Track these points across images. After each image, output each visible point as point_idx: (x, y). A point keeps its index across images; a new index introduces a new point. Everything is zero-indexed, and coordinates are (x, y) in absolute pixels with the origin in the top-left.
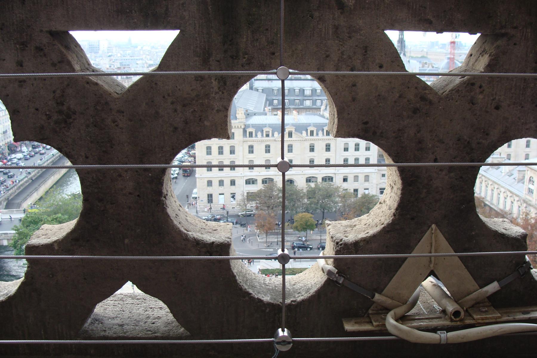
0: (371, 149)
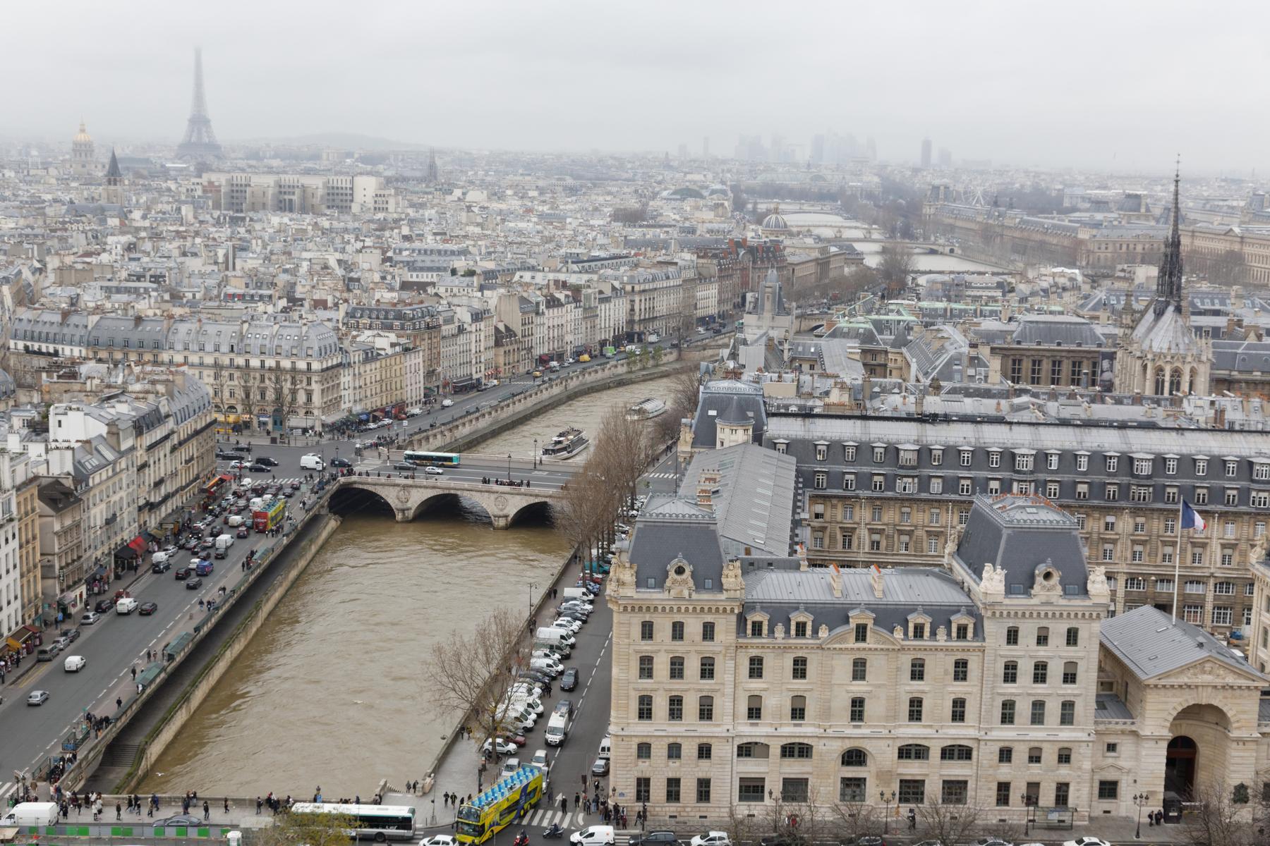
0: (1078, 678)
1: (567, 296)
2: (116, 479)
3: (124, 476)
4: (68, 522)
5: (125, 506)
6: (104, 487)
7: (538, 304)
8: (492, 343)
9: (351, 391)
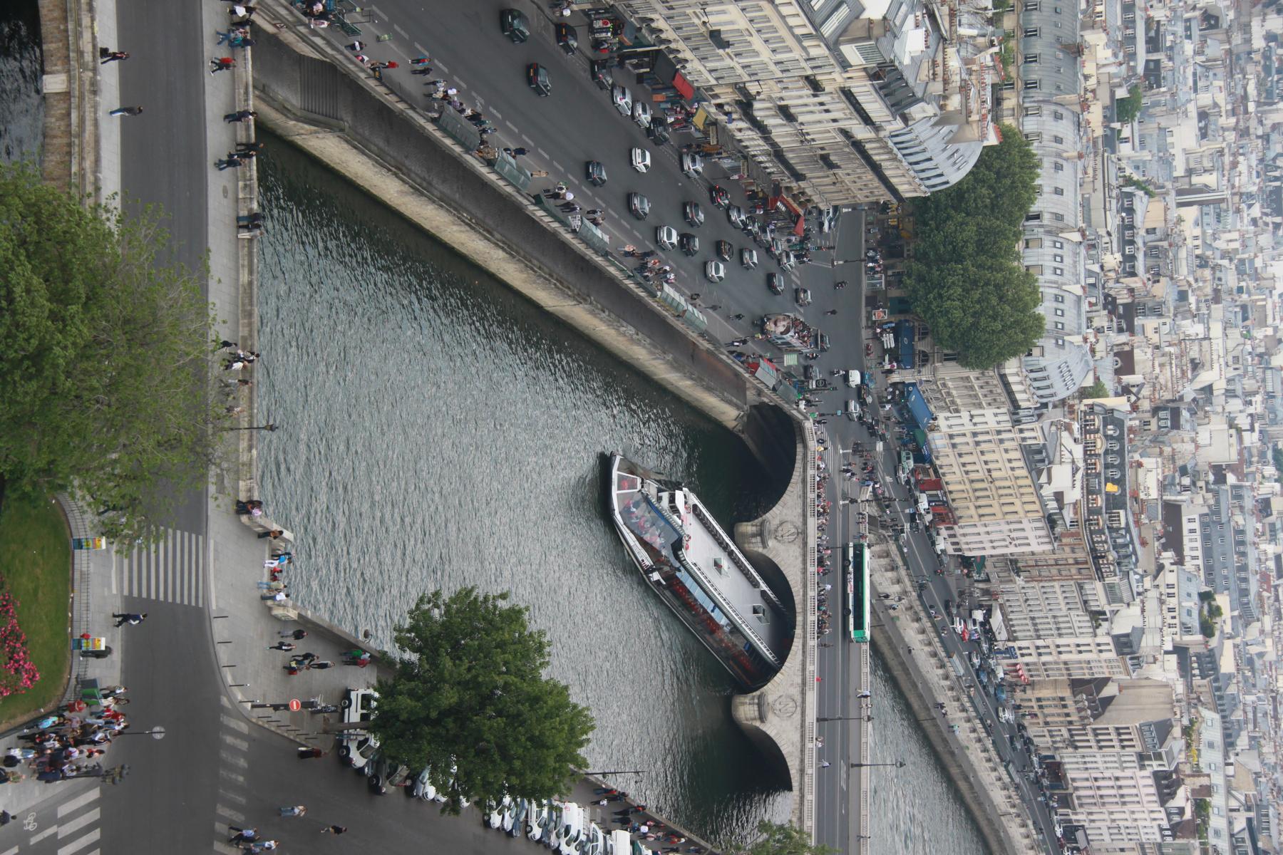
1: (1181, 811)
2: (791, 42)
3: (797, 54)
5: (745, 61)
6: (776, 21)
8: (1077, 675)
9: (969, 428)
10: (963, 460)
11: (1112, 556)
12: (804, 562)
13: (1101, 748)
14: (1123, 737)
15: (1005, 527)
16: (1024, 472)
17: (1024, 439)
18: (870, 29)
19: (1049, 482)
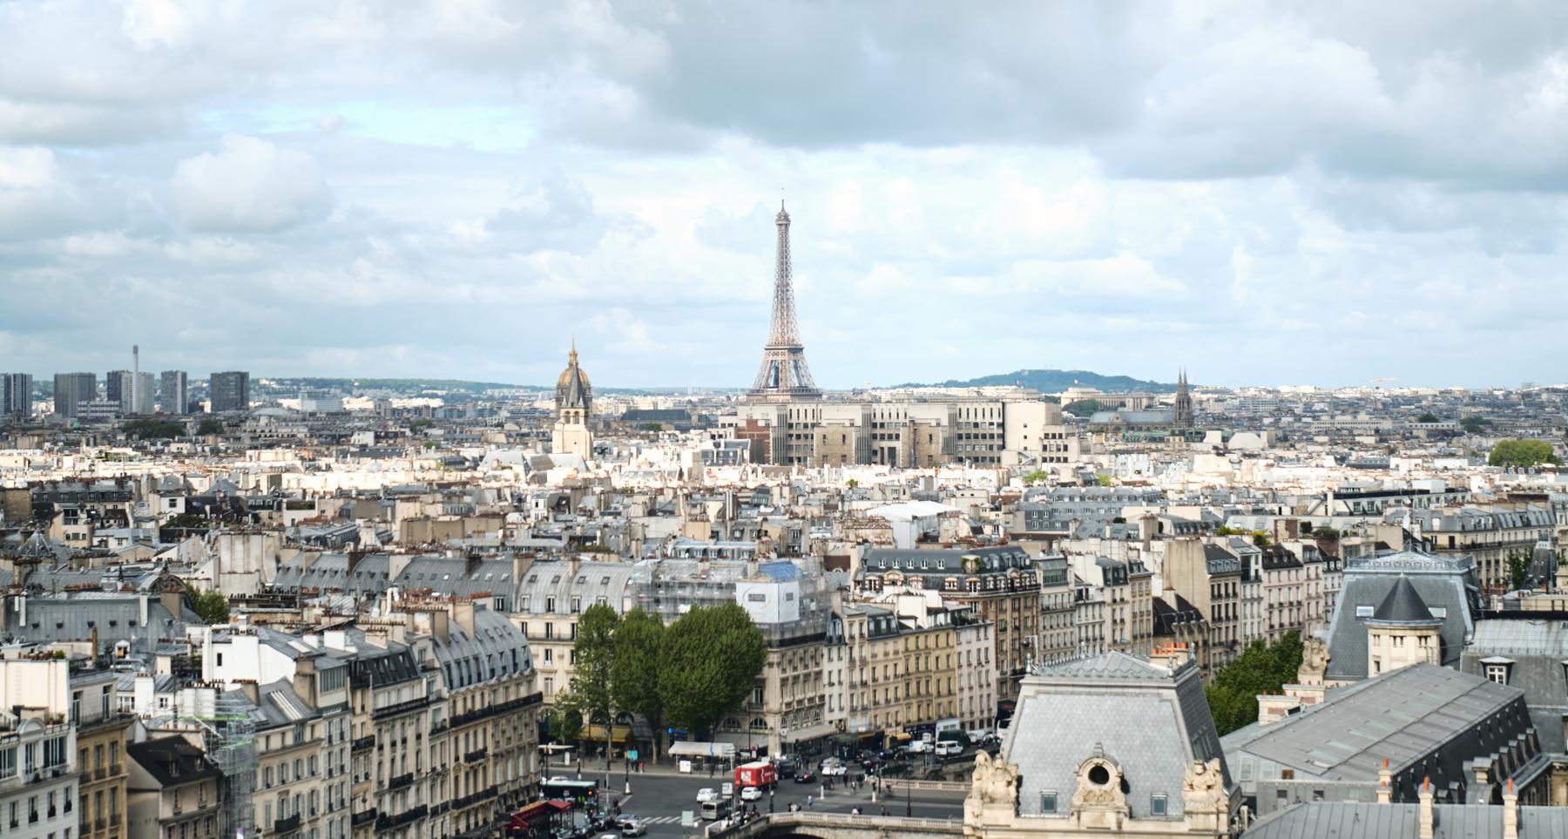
1: (1306, 549)
2: (304, 755)
4: (189, 807)
5: (322, 808)
7: (1246, 561)
8: (1148, 626)
9: (845, 690)
10: (882, 701)
11: (1010, 573)
12: (917, 831)
13: (1235, 617)
14: (1223, 592)
15: (965, 670)
16: (901, 644)
17: (862, 635)
18: (305, 676)
19: (915, 618)
